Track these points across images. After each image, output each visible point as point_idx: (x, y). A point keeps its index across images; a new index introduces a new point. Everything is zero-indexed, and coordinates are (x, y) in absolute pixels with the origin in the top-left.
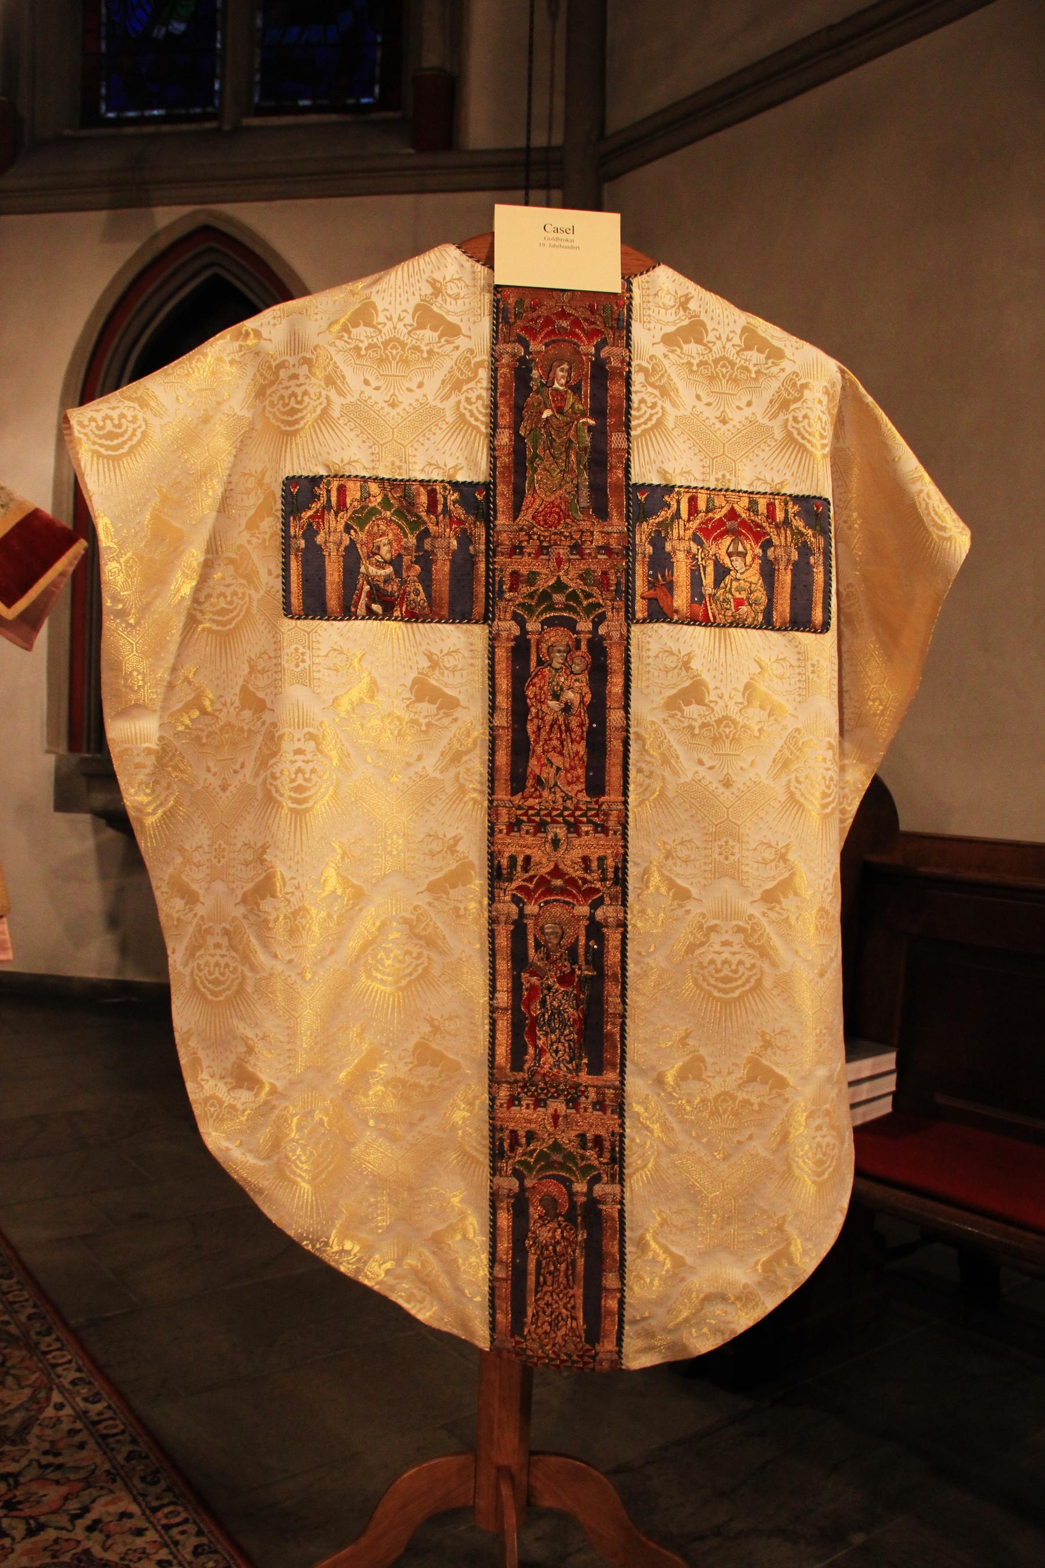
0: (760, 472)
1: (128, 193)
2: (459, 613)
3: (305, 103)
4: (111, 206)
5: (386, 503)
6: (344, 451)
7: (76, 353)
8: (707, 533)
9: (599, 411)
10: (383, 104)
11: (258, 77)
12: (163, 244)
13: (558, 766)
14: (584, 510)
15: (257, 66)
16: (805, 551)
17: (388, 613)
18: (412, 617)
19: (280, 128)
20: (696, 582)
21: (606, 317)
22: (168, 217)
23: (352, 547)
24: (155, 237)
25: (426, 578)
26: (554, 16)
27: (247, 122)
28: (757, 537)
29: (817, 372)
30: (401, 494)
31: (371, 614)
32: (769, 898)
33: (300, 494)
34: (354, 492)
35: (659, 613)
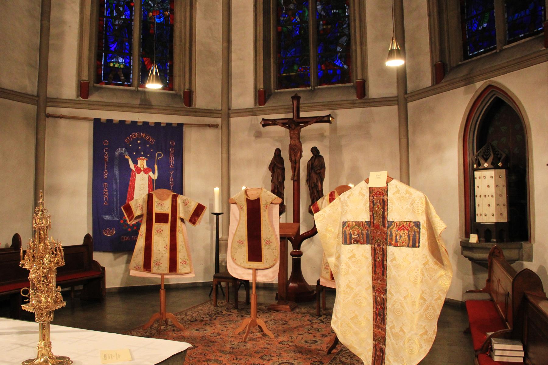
0: (408, 218)
1: (468, 81)
2: (368, 243)
5: (356, 225)
6: (351, 218)
8: (399, 229)
9: (383, 208)
11: (507, 32)
12: (478, 93)
13: (378, 270)
15: (507, 29)
16: (415, 232)
17: (357, 243)
18: (361, 243)
19: (512, 47)
20: (396, 239)
22: (479, 85)
23: (350, 233)
24: (477, 91)
25: (363, 237)
27: (504, 47)
28: (407, 230)
30: (358, 224)
31: (354, 243)
32: (405, 298)
33: (344, 223)
34: (351, 224)
35: (391, 245)
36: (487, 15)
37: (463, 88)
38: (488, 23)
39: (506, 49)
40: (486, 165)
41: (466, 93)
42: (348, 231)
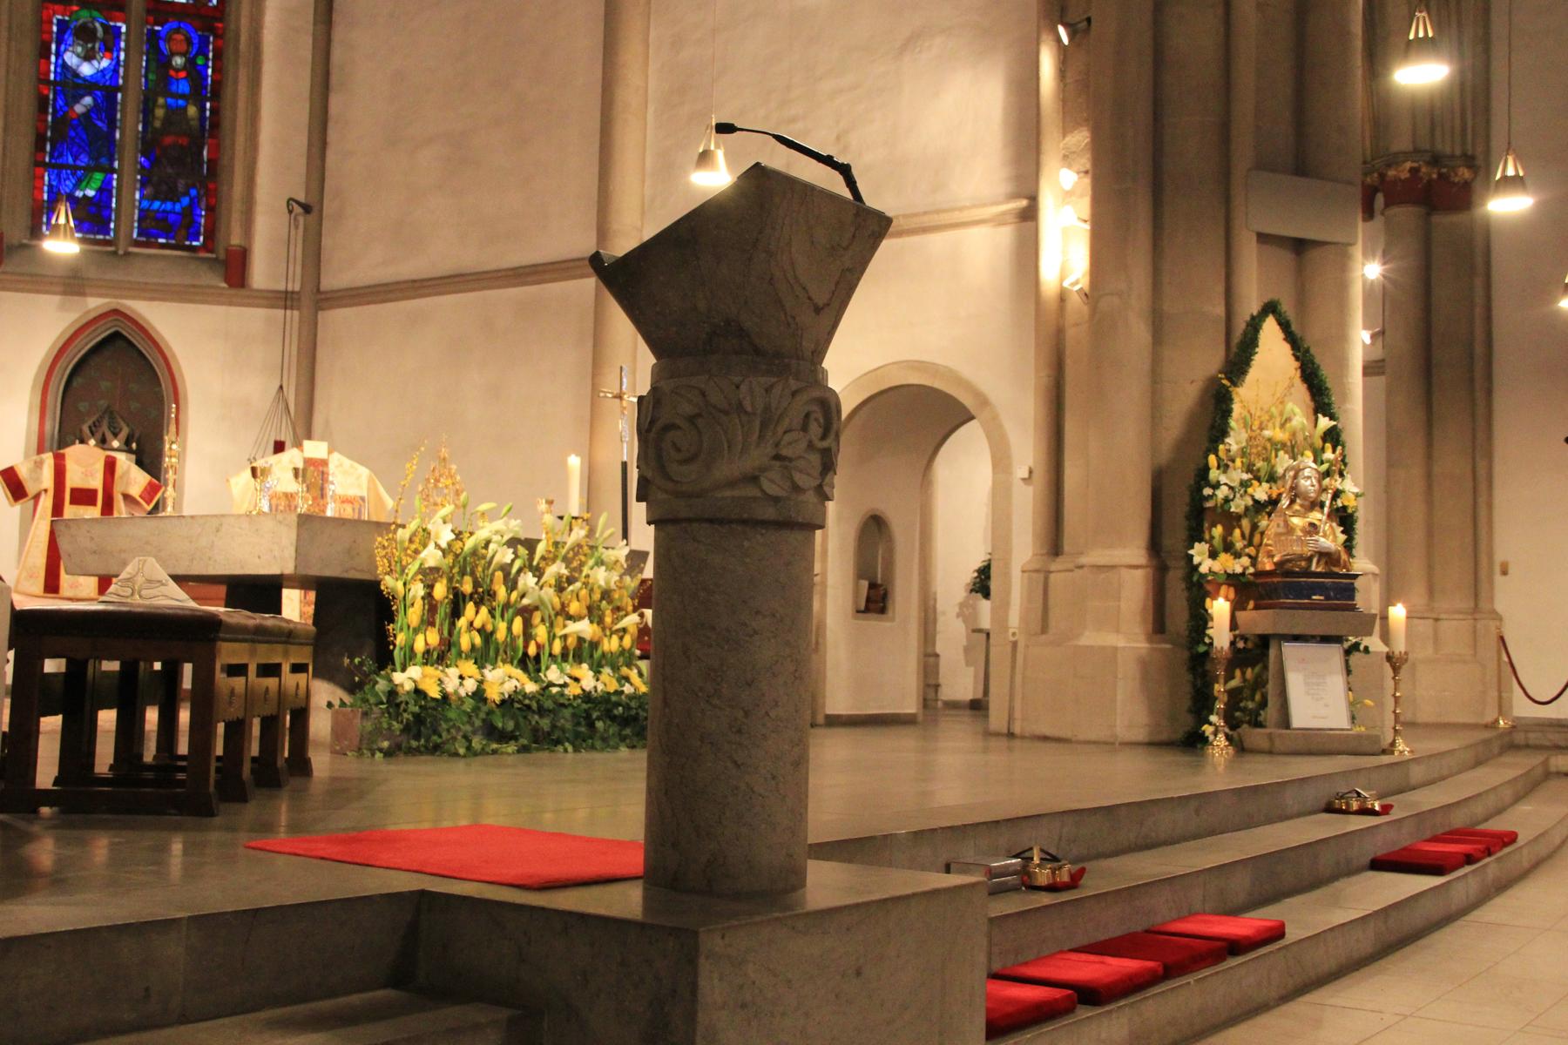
0: (352, 492)
3: (162, 241)
4: (64, 293)
7: (40, 367)
10: (205, 247)
14: (314, 475)
21: (324, 463)
22: (95, 304)
26: (297, 227)
29: (364, 472)
36: (99, 176)
37: (57, 298)
38: (100, 191)
39: (137, 255)
40: (116, 444)
41: (62, 308)
42: (274, 502)
